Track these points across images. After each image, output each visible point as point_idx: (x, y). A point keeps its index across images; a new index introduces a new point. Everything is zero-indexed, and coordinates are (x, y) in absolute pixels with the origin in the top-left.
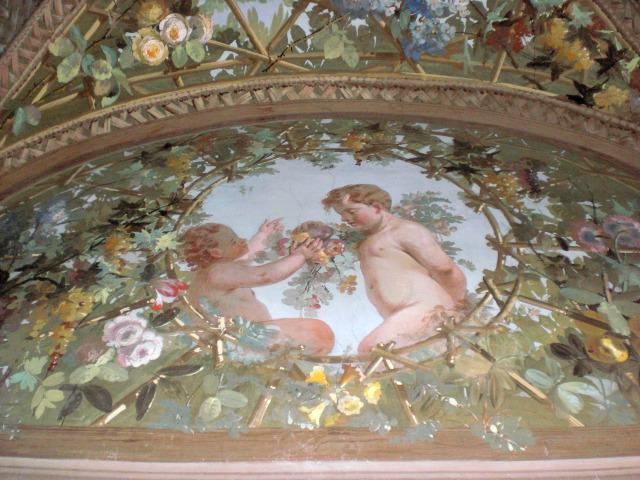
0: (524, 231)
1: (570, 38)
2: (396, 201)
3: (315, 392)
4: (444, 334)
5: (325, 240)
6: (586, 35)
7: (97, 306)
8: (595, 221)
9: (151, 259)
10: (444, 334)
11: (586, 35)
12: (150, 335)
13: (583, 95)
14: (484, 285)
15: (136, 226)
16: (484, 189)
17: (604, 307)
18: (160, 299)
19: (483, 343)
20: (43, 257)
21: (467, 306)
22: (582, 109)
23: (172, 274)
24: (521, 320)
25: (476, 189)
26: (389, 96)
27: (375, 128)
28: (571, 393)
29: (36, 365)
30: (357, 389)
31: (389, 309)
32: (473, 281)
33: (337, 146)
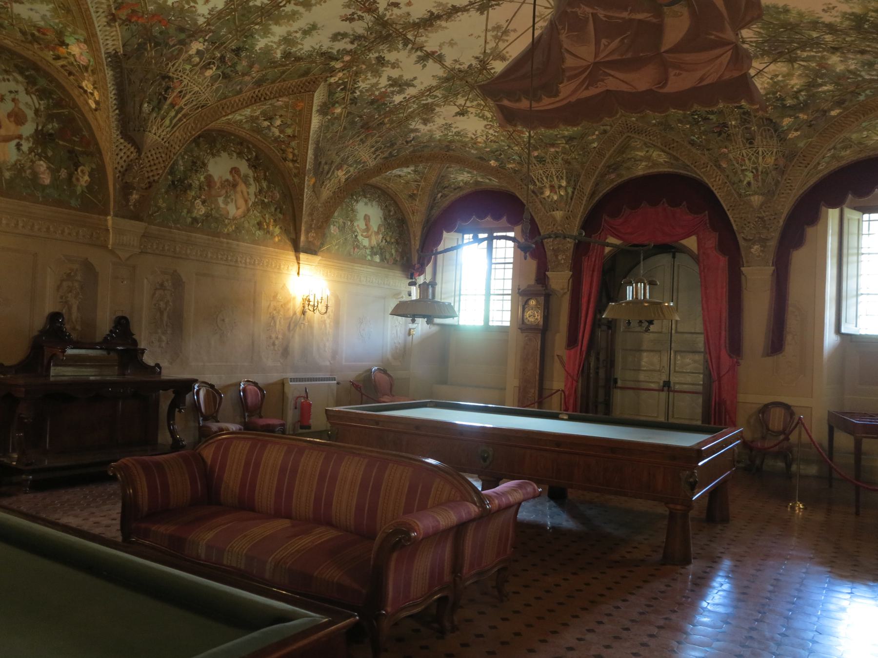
0: (260, 191)
1: (291, 152)
2: (242, 176)
3: (226, 226)
4: (244, 217)
5: (229, 185)
6: (294, 155)
7: (193, 196)
8: (272, 191)
9: (200, 184)
10: (244, 217)
11: (294, 155)
12: (202, 207)
13: (285, 159)
14: (251, 206)
15: (196, 171)
16: (257, 175)
17: (267, 216)
18: (203, 197)
19: (249, 220)
20: (180, 178)
21: (248, 210)
22: (283, 161)
23: (204, 189)
24: (255, 216)
25: (256, 175)
26: (248, 136)
27: (241, 144)
28: (258, 233)
29: (185, 211)
30: (231, 226)
31: (238, 208)
32: (250, 203)
33: (233, 149)
